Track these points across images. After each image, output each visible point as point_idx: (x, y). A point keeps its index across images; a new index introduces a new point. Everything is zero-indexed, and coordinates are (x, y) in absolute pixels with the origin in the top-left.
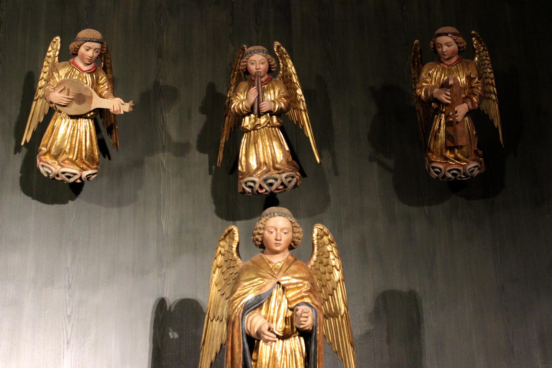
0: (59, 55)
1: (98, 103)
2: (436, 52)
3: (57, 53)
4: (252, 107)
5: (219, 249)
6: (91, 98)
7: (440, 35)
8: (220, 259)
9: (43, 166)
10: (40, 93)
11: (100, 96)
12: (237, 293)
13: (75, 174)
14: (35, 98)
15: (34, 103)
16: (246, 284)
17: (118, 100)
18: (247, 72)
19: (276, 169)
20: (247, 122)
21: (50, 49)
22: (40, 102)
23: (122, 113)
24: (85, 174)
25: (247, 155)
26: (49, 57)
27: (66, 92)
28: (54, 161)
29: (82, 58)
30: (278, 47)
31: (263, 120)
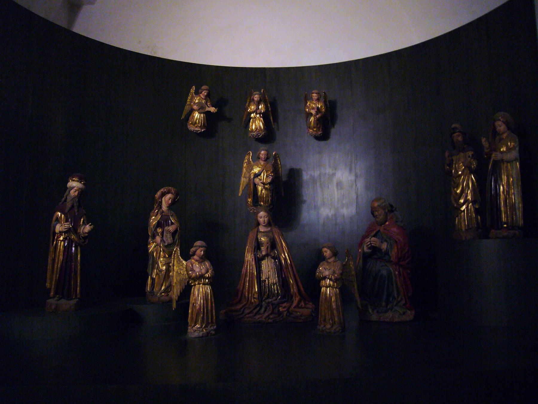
0: (194, 92)
1: (208, 109)
2: (312, 97)
3: (194, 91)
4: (255, 111)
5: (246, 157)
6: (205, 108)
7: (313, 93)
8: (246, 160)
9: (190, 128)
10: (188, 103)
11: (208, 107)
12: (252, 171)
13: (199, 130)
14: (187, 105)
15: (186, 106)
16: (254, 169)
17: (214, 108)
18: (253, 100)
19: (261, 131)
20: (252, 115)
21: (191, 90)
22: (188, 106)
23: (215, 112)
24: (203, 130)
25: (252, 126)
26: (191, 92)
27: (198, 106)
28: (193, 126)
29: (203, 95)
30: (263, 91)
31: (258, 115)
